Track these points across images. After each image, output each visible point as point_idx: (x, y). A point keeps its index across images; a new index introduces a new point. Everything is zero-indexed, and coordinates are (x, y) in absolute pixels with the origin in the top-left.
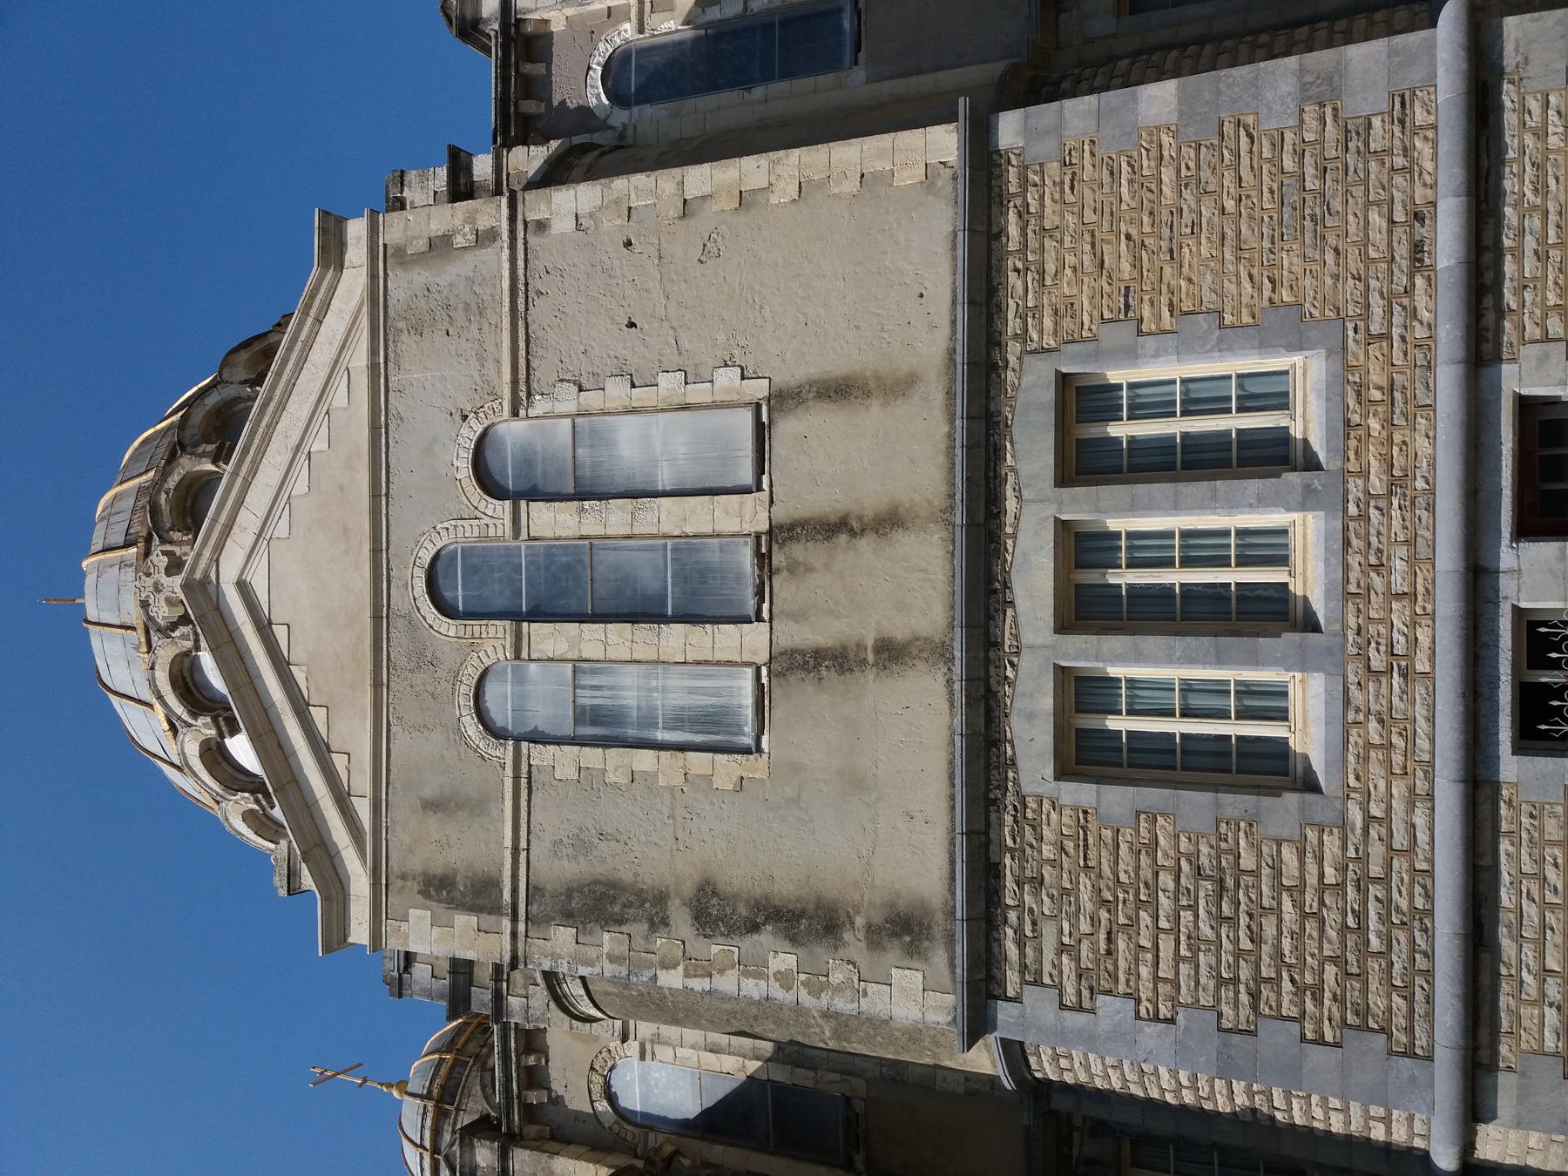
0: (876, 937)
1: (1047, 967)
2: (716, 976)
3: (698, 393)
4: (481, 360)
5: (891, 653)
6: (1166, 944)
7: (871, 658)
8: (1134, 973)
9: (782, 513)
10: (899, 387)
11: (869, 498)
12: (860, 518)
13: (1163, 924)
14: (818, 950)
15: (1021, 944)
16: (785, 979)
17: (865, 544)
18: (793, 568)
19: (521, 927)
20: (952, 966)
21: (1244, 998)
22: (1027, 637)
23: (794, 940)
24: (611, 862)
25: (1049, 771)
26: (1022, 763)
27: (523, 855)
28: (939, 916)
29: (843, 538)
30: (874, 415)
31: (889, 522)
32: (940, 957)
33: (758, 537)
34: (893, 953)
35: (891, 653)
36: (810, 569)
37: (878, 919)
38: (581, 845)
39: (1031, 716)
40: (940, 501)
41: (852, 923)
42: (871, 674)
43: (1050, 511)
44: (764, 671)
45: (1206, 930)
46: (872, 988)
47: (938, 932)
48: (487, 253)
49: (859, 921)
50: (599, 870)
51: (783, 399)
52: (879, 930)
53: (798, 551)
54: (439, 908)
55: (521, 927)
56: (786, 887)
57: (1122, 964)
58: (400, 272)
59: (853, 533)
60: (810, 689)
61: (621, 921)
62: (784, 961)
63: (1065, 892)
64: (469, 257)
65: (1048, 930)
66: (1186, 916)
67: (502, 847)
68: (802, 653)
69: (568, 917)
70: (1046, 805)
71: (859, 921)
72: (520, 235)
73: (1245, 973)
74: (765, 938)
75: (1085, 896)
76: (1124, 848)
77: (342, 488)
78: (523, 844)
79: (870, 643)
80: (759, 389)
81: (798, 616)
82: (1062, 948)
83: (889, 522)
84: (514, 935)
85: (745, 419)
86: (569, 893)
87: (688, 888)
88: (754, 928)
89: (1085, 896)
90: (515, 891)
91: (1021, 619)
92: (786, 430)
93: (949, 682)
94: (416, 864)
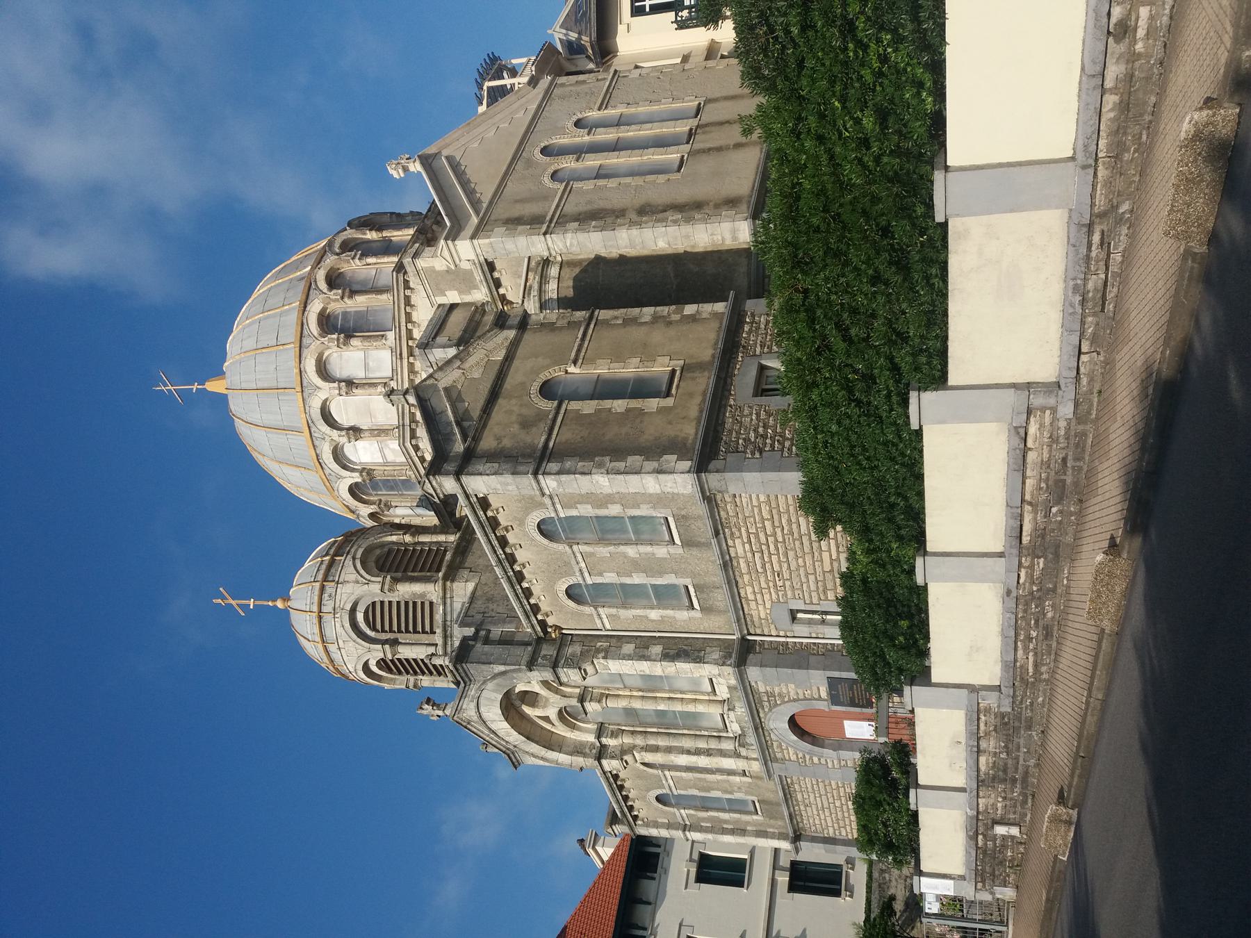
19: (553, 225)
20: (748, 208)
27: (560, 208)
29: (726, 125)
32: (744, 207)
36: (711, 132)
41: (708, 204)
67: (550, 207)
86: (580, 214)
93: (762, 149)
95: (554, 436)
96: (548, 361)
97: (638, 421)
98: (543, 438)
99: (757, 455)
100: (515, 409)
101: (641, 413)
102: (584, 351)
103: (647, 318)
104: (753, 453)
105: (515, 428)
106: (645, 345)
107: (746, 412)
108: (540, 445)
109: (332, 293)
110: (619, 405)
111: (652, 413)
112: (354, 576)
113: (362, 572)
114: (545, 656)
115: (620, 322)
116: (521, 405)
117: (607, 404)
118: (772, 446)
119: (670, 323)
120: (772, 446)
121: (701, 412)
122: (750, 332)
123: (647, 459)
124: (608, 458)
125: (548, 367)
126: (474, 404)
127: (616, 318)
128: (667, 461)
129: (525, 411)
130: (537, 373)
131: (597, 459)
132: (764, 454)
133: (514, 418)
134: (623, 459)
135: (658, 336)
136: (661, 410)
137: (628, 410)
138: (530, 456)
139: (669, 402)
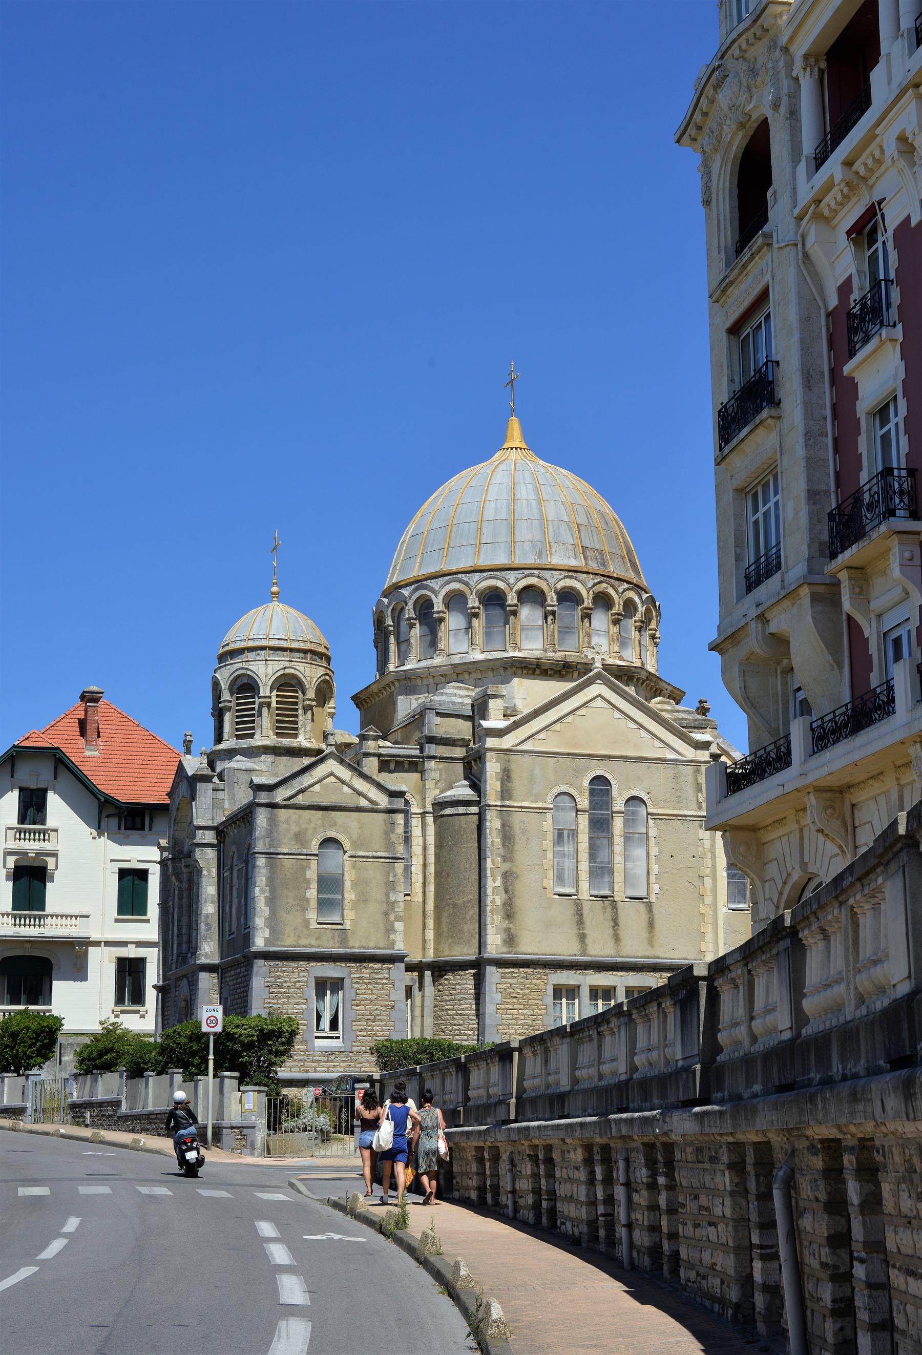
0: (508, 930)
1: (506, 980)
2: (491, 878)
3: (653, 878)
4: (665, 801)
5: (582, 938)
6: (515, 1012)
7: (581, 932)
8: (507, 1003)
9: (619, 905)
10: (651, 942)
11: (622, 933)
12: (618, 929)
13: (520, 1011)
14: (502, 913)
15: (510, 973)
16: (493, 902)
17: (611, 931)
18: (604, 908)
19: (499, 809)
21: (505, 1031)
22: (588, 978)
23: (504, 904)
24: (520, 841)
25: (555, 983)
26: (556, 975)
27: (520, 810)
28: (515, 950)
29: (612, 924)
30: (644, 934)
31: (617, 939)
32: (505, 950)
33: (612, 897)
34: (505, 936)
35: (582, 938)
36: (604, 913)
37: (513, 931)
38: (524, 832)
39: (568, 978)
40: (621, 954)
42: (576, 932)
43: (619, 985)
44: (576, 897)
45: (520, 1022)
46: (495, 929)
47: (511, 949)
48: (695, 806)
49: (511, 926)
50: (517, 838)
51: (649, 906)
52: (510, 932)
53: (609, 909)
54: (500, 776)
55: (499, 809)
56: (519, 903)
57: (509, 1000)
58: (691, 771)
59: (614, 927)
60: (572, 912)
61: (503, 845)
62: (499, 902)
63: (525, 985)
64: (694, 799)
65: (514, 981)
66: (522, 1017)
68: (582, 909)
69: (503, 825)
70: (546, 981)
71: (511, 926)
72: (699, 819)
73: (511, 1031)
74: (504, 896)
75: (525, 991)
76: (537, 1001)
77: (628, 742)
78: (523, 810)
79: (585, 932)
80: (653, 899)
81: (591, 909)
82: (511, 984)
83: (617, 939)
84: (496, 806)
85: (643, 894)
87: (515, 869)
88: (506, 892)
89: (525, 991)
90: (509, 807)
91: (591, 976)
92: (641, 907)
93: (575, 955)
94: (513, 767)
95: (287, 857)
96: (355, 836)
97: (298, 908)
98: (285, 851)
99: (266, 984)
100: (313, 825)
101: (304, 910)
102: (364, 860)
103: (392, 897)
104: (268, 982)
105: (294, 829)
106: (366, 901)
107: (301, 974)
108: (279, 850)
109: (514, 594)
110: (312, 893)
111: (304, 915)
112: (270, 671)
113: (274, 678)
114: (204, 834)
115: (391, 879)
116: (315, 828)
117: (314, 886)
118: (273, 993)
119: (386, 914)
120: (273, 993)
121: (304, 947)
122: (372, 968)
123: (266, 919)
124: (267, 894)
125: (350, 838)
126: (317, 795)
127: (395, 876)
128: (264, 932)
129: (310, 832)
130: (346, 831)
131: (268, 888)
132: (268, 988)
133: (304, 826)
134: (267, 904)
135: (374, 909)
136: (307, 923)
137: (308, 900)
138: (270, 845)
139: (314, 925)
